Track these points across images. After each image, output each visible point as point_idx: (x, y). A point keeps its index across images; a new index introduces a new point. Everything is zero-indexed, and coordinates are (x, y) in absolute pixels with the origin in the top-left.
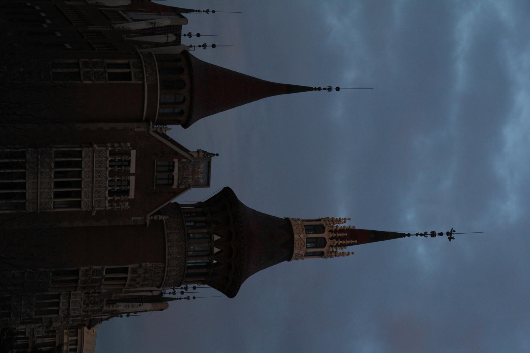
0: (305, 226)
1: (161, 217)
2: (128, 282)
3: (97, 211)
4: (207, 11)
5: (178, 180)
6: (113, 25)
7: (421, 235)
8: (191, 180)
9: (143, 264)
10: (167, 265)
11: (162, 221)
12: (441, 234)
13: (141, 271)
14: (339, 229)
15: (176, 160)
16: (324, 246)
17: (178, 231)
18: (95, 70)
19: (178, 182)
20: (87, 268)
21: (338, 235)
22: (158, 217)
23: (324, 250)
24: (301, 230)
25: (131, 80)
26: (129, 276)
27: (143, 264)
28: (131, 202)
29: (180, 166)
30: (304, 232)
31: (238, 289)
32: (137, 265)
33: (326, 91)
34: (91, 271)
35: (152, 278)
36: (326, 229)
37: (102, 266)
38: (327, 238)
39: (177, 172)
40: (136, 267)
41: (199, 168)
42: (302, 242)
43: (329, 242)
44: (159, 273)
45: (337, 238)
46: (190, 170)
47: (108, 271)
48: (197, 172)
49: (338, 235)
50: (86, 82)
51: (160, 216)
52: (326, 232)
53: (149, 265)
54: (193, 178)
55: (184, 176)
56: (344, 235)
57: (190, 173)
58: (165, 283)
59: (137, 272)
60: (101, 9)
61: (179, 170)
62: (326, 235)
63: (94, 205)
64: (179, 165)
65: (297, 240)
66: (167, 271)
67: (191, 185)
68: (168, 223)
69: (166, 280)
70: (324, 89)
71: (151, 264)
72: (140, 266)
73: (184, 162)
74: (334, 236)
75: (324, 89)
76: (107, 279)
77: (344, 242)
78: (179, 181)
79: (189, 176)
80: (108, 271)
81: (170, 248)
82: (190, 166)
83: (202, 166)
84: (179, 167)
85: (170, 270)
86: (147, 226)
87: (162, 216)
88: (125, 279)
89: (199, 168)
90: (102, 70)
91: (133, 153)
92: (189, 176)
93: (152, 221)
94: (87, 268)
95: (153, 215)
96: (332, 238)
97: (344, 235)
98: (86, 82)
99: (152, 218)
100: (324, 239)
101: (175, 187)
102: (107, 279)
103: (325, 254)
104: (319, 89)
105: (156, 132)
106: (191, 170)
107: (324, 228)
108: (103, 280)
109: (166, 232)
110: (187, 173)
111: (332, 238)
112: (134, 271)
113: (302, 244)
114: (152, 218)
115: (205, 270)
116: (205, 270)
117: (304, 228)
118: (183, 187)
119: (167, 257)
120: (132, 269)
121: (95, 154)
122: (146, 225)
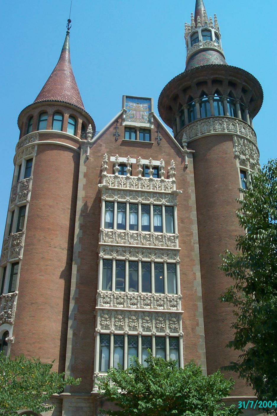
0: (192, 45)
1: (185, 139)
3: (176, 189)
5: (145, 123)
8: (145, 112)
10: (236, 133)
13: (243, 157)
15: (125, 123)
16: (210, 31)
17: (199, 126)
18: (18, 191)
22: (185, 142)
23: (213, 31)
25: (33, 156)
28: (168, 163)
29: (130, 120)
30: (197, 44)
39: (136, 123)
40: (239, 160)
42: (207, 43)
44: (244, 143)
46: (135, 113)
48: (137, 108)
50: (29, 198)
51: (183, 141)
52: (197, 30)
55: (141, 118)
57: (138, 113)
59: (244, 159)
61: (134, 121)
63: (170, 192)
64: (128, 121)
66: (241, 134)
67: (150, 112)
68: (191, 137)
70: (69, 29)
73: (126, 116)
75: (69, 29)
79: (141, 114)
81: (217, 130)
82: (130, 112)
84: (131, 121)
85: (240, 132)
86: (194, 151)
87: (183, 139)
90: (19, 184)
91: (113, 159)
92: (141, 114)
93: (188, 147)
95: (183, 147)
98: (29, 198)
99: (185, 147)
104: (68, 33)
105: (92, 138)
106: (135, 112)
109: (200, 135)
110: (138, 115)
112: (243, 162)
113: (208, 44)
114: (185, 147)
115: (238, 106)
120: (240, 165)
121: (109, 187)
122: (193, 153)
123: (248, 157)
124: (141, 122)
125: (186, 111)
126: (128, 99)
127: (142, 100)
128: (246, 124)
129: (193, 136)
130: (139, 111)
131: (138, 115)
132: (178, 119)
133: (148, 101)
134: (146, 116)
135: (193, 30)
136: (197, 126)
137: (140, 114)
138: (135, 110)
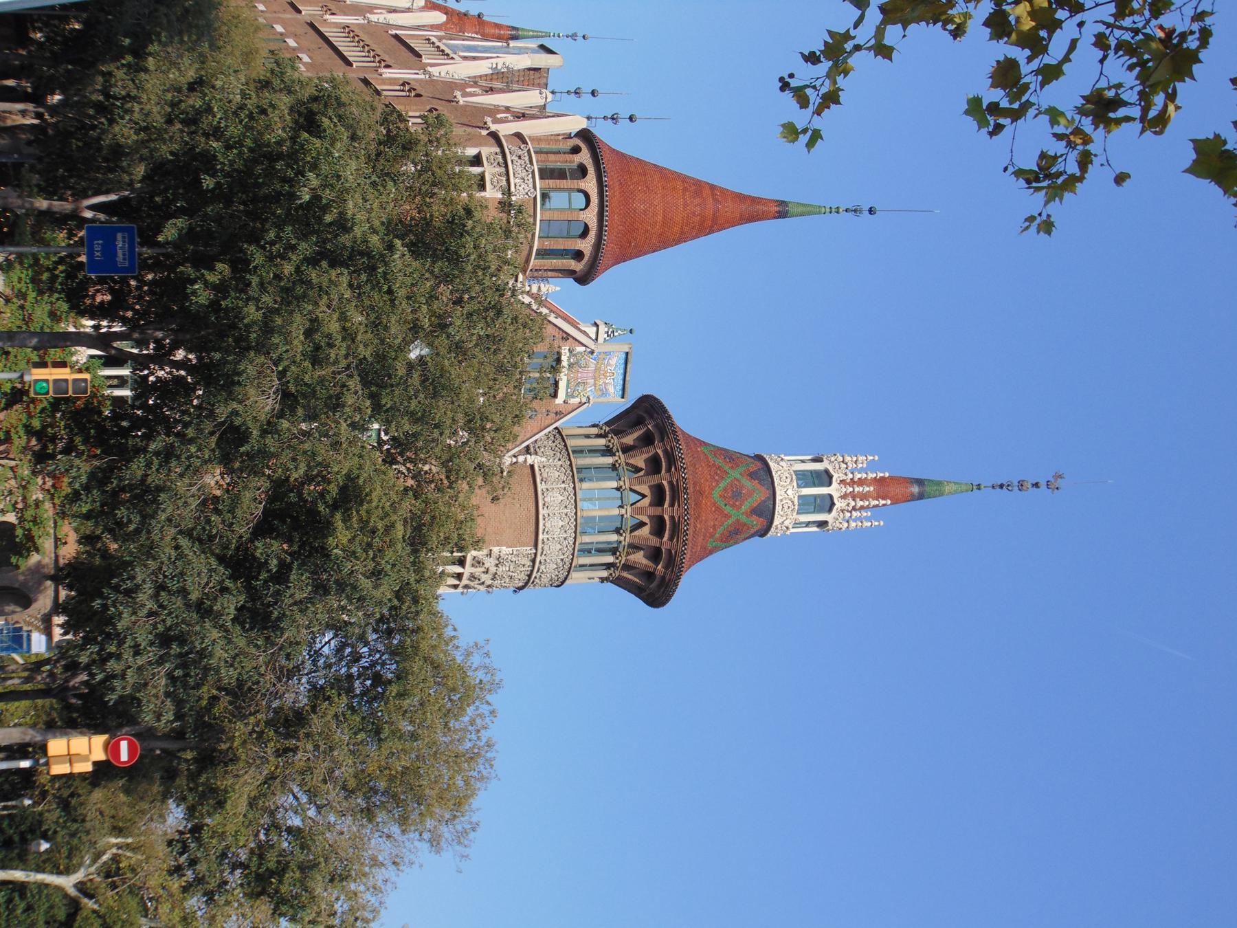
1: (530, 459)
2: (465, 581)
4: (573, 36)
5: (568, 387)
6: (429, 69)
7: (1001, 486)
9: (496, 550)
11: (532, 467)
12: (1036, 485)
13: (490, 563)
14: (859, 479)
16: (830, 510)
17: (563, 486)
19: (567, 392)
21: (857, 489)
24: (789, 480)
26: (468, 570)
27: (496, 550)
31: (670, 597)
33: (850, 214)
35: (511, 574)
36: (834, 479)
38: (836, 496)
41: (608, 364)
43: (839, 504)
45: (854, 496)
49: (857, 489)
52: (835, 484)
53: (505, 550)
54: (595, 385)
56: (868, 489)
58: (533, 582)
60: (398, 32)
62: (834, 490)
65: (781, 500)
66: (540, 563)
68: (542, 470)
69: (536, 577)
71: (510, 549)
72: (490, 554)
74: (848, 492)
77: (867, 503)
78: (569, 390)
83: (613, 361)
89: (608, 364)
96: (844, 497)
97: (868, 489)
99: (514, 460)
100: (831, 497)
101: (560, 400)
103: (830, 524)
106: (592, 368)
107: (831, 477)
110: (585, 375)
111: (844, 497)
116: (610, 559)
117: (794, 476)
118: (576, 401)
119: (541, 537)
123: (493, 569)
124: (568, 381)
125: (609, 460)
126: (624, 356)
127: (621, 382)
128: (569, 572)
129: (545, 475)
130: (595, 378)
131: (585, 375)
132: (602, 441)
133: (620, 393)
134: (584, 390)
135: (835, 476)
136: (563, 482)
137: (587, 378)
138: (597, 369)
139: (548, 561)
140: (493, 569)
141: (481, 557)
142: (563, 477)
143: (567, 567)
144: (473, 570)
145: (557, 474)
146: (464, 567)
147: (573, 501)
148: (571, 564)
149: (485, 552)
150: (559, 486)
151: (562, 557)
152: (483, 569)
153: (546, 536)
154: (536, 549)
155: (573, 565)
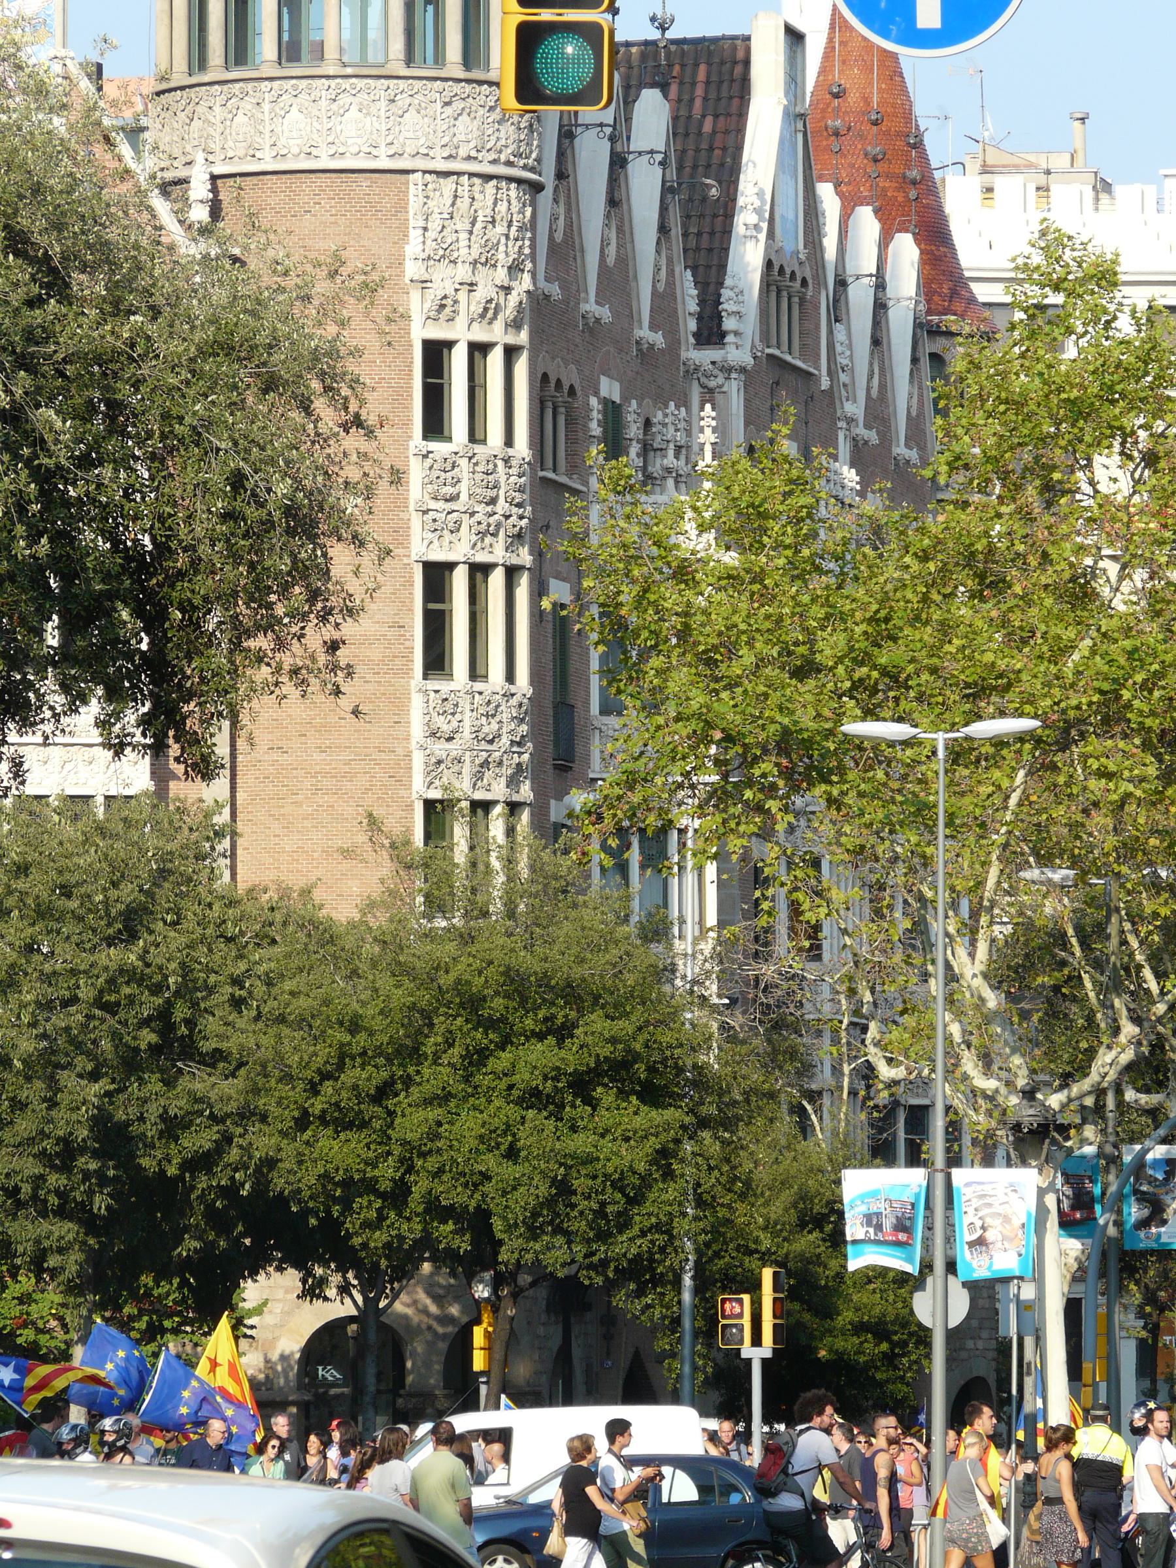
13: (445, 279)
17: (266, 107)
20: (416, 521)
27: (412, 270)
32: (415, 296)
34: (433, 505)
37: (412, 459)
47: (435, 425)
53: (414, 246)
58: (509, 163)
76: (476, 436)
80: (435, 425)
88: (479, 350)
94: (416, 521)
102: (476, 436)
108: (478, 449)
129: (241, 153)
139: (446, 140)
140: (463, 272)
141: (427, 305)
142: (247, 104)
143: (468, 88)
144: (462, 321)
145: (240, 119)
146: (450, 344)
147: (303, 83)
148: (459, 81)
149: (415, 296)
150: (267, 117)
151: (439, 104)
152: (462, 296)
153: (383, 151)
154: (414, 171)
155: (462, 74)
